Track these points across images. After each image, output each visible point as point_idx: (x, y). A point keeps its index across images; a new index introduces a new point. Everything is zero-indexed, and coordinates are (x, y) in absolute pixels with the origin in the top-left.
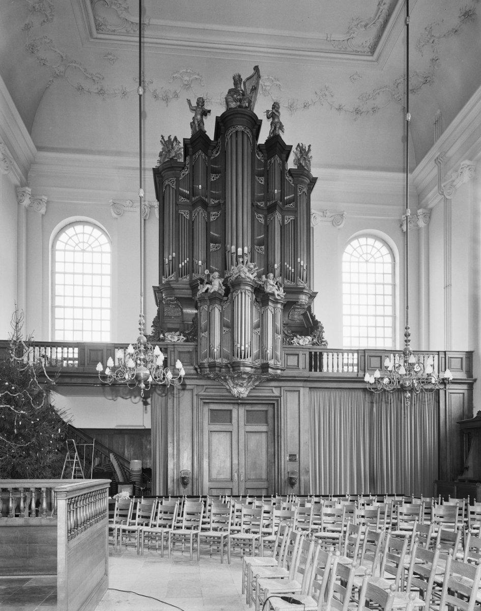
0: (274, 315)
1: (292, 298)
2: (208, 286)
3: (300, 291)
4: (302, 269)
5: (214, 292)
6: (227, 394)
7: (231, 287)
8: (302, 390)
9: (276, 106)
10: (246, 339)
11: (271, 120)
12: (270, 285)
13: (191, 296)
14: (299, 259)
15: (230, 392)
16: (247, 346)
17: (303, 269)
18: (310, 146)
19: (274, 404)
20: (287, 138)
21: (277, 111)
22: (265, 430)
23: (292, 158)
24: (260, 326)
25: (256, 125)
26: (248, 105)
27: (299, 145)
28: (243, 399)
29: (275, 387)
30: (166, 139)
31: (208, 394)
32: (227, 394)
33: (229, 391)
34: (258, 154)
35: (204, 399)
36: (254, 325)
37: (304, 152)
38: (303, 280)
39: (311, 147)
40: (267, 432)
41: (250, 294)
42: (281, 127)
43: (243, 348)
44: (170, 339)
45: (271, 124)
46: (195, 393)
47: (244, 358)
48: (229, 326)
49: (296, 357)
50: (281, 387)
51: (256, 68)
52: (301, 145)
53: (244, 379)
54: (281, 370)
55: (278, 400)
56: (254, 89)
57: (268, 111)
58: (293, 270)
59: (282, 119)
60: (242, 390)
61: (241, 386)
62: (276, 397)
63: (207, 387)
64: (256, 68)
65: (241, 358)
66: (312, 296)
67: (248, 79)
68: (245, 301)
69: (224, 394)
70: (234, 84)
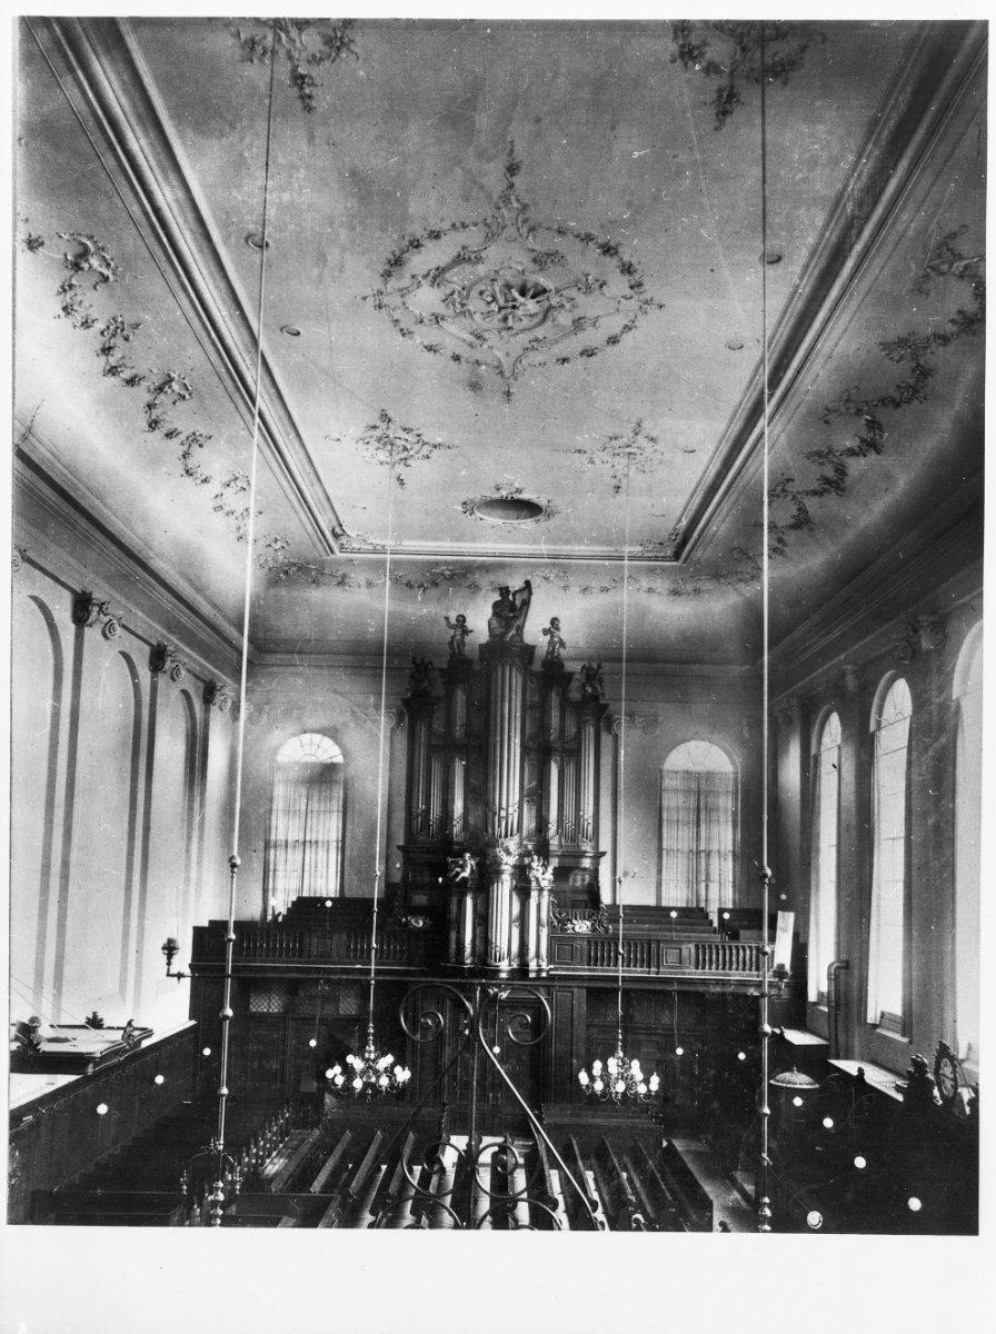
1: (569, 862)
2: (459, 870)
3: (583, 855)
5: (464, 878)
9: (554, 621)
10: (504, 936)
23: (574, 684)
30: (418, 662)
45: (549, 643)
48: (484, 920)
56: (526, 603)
66: (598, 856)
68: (504, 889)
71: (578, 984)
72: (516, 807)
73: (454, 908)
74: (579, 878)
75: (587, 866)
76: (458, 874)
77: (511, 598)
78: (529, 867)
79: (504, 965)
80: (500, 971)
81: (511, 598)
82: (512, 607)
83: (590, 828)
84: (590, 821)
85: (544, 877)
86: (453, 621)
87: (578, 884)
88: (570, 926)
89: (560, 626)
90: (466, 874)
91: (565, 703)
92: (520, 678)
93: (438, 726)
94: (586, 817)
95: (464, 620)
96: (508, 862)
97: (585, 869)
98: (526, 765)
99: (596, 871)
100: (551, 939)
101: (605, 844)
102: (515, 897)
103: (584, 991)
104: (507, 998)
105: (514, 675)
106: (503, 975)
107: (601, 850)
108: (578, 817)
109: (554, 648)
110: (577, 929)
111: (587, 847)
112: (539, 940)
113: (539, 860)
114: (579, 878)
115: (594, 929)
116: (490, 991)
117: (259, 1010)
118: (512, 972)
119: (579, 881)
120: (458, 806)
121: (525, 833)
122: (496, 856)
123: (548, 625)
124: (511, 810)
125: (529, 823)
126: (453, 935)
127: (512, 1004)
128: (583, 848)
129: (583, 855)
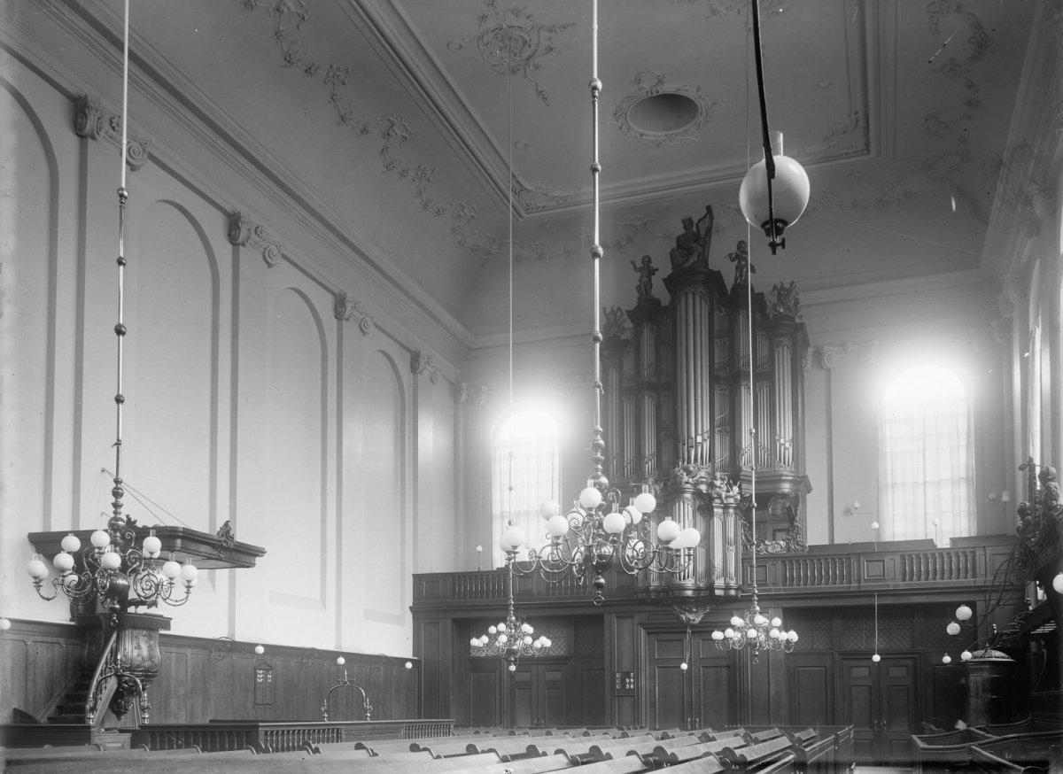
1: (767, 488)
4: (783, 447)
11: (736, 262)
14: (777, 438)
18: (792, 283)
25: (715, 279)
27: (775, 288)
28: (693, 626)
34: (720, 311)
38: (784, 463)
40: (728, 666)
47: (684, 579)
51: (709, 208)
52: (779, 285)
56: (709, 231)
57: (730, 255)
60: (691, 617)
61: (690, 612)
64: (709, 208)
65: (680, 579)
72: (706, 436)
74: (779, 506)
75: (786, 491)
79: (690, 583)
80: (684, 588)
81: (695, 230)
82: (697, 238)
84: (787, 445)
86: (639, 264)
87: (779, 512)
92: (706, 308)
94: (782, 441)
97: (784, 496)
98: (716, 396)
102: (698, 515)
106: (689, 593)
108: (773, 442)
114: (779, 506)
118: (697, 590)
124: (699, 439)
125: (721, 455)
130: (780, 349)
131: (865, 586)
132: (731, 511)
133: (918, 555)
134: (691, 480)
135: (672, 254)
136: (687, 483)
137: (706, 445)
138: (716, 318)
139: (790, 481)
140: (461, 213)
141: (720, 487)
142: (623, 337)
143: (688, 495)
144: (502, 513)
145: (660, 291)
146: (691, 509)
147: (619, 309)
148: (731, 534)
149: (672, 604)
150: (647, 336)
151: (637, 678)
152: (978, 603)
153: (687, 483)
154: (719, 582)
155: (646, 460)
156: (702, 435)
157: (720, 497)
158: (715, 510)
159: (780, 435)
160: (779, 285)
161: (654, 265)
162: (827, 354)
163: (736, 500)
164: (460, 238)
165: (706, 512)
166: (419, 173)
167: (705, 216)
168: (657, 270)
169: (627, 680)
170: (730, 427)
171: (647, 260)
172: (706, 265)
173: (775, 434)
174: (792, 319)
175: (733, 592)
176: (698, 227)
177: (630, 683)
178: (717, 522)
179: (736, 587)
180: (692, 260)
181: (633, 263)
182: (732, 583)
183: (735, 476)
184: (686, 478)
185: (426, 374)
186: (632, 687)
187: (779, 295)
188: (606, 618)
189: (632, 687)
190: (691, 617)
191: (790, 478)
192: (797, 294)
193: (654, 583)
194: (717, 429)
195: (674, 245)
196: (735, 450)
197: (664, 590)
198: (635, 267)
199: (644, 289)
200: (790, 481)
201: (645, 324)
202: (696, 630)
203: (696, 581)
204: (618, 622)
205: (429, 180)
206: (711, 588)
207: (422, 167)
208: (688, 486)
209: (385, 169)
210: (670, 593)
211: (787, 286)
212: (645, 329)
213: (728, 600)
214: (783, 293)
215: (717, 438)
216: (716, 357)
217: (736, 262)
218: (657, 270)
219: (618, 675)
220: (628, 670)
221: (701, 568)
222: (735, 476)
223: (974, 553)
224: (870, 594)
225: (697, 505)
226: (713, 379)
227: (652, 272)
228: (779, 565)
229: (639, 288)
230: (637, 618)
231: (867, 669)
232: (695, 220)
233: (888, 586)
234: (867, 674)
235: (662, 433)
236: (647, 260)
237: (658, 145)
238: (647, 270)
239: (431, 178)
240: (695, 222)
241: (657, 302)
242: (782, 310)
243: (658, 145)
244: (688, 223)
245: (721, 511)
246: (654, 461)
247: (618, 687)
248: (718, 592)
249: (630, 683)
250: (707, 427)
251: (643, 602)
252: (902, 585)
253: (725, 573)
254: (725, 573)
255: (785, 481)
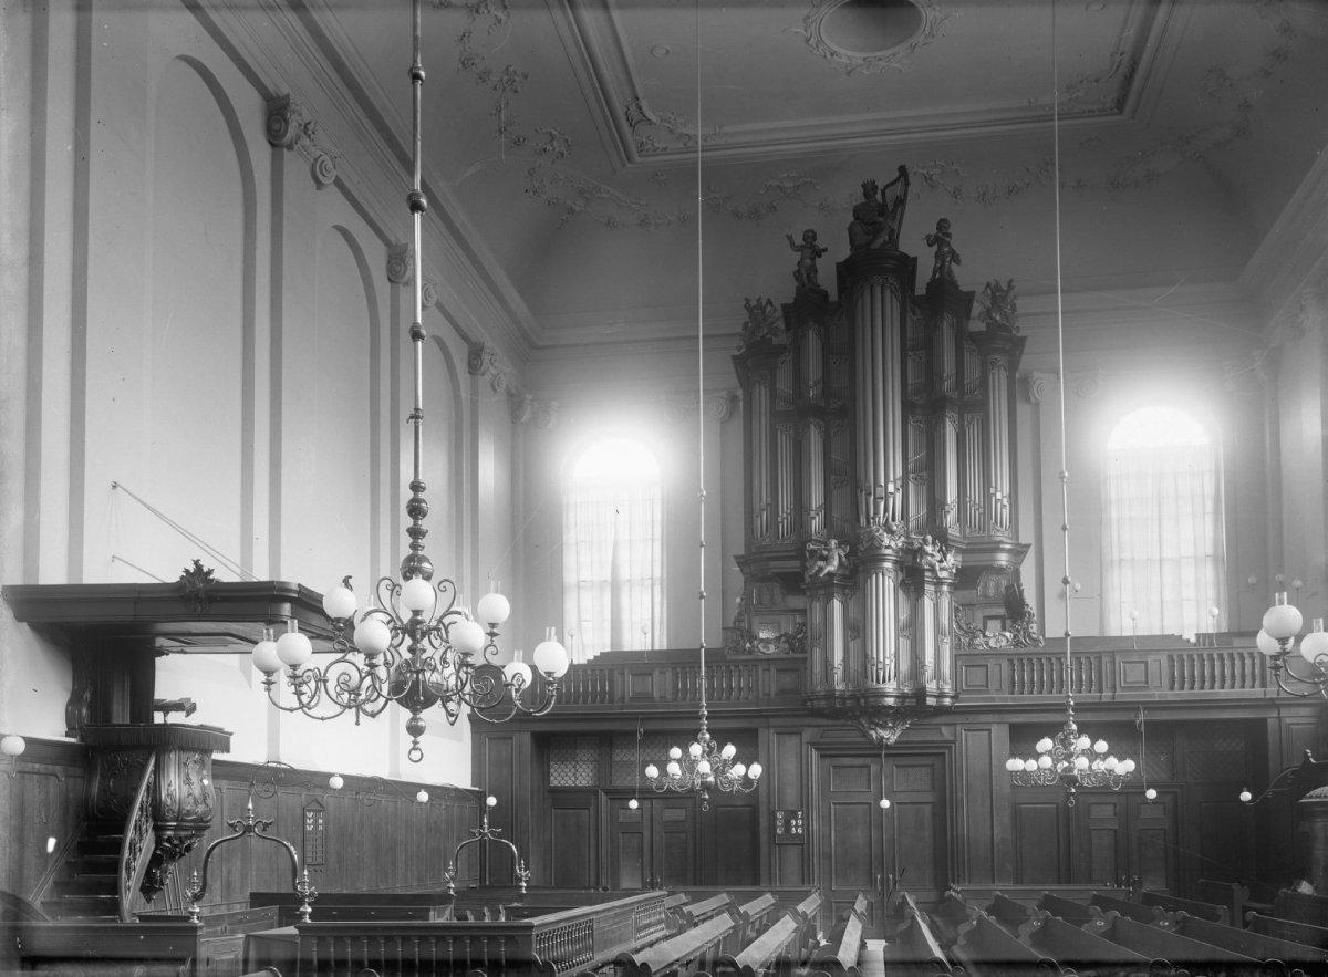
0: (937, 609)
1: (977, 560)
3: (995, 548)
5: (829, 574)
6: (863, 740)
7: (862, 563)
8: (994, 728)
10: (888, 646)
11: (935, 247)
12: (927, 554)
13: (799, 570)
14: (992, 491)
15: (865, 736)
16: (887, 662)
17: (1003, 506)
19: (943, 754)
20: (967, 276)
21: (949, 235)
22: (931, 800)
23: (977, 309)
24: (911, 629)
25: (907, 266)
26: (890, 239)
27: (988, 285)
28: (888, 747)
29: (945, 724)
31: (827, 740)
32: (863, 740)
33: (865, 735)
35: (823, 749)
36: (901, 624)
37: (1000, 295)
38: (1001, 526)
39: (1014, 284)
40: (933, 803)
41: (892, 575)
42: (955, 258)
43: (880, 666)
44: (762, 649)
46: (804, 741)
47: (884, 681)
48: (858, 629)
49: (984, 669)
50: (955, 724)
51: (903, 170)
52: (993, 283)
53: (888, 715)
54: (952, 697)
55: (943, 754)
56: (900, 202)
57: (928, 236)
58: (981, 510)
59: (955, 243)
60: (885, 734)
61: (884, 727)
62: (945, 742)
63: (826, 728)
64: (903, 170)
65: (878, 681)
66: (1019, 552)
67: (887, 186)
68: (885, 589)
69: (859, 739)
70: (865, 194)
71: (996, 717)
72: (899, 483)
73: (817, 619)
75: (1004, 563)
76: (821, 569)
77: (879, 196)
78: (921, 552)
79: (890, 687)
80: (885, 695)
81: (879, 196)
83: (1006, 512)
84: (1005, 501)
85: (945, 564)
86: (799, 241)
87: (991, 592)
88: (980, 640)
89: (950, 231)
90: (832, 567)
91: (962, 336)
92: (897, 306)
93: (784, 384)
94: (999, 496)
95: (814, 238)
96: (891, 545)
97: (1000, 570)
99: (1017, 573)
100: (956, 658)
101: (1027, 536)
102: (900, 592)
103: (1006, 727)
104: (897, 742)
105: (888, 299)
106: (890, 701)
107: (1023, 541)
109: (943, 262)
110: (992, 643)
111: (1002, 536)
112: (937, 656)
113: (934, 544)
115: (1017, 643)
116: (873, 733)
117: (563, 783)
118: (901, 697)
119: (992, 586)
120: (816, 498)
121: (912, 524)
122: (872, 538)
123: (934, 232)
124: (891, 488)
125: (917, 511)
126: (817, 654)
127: (898, 753)
128: (998, 539)
129: (995, 548)
130: (996, 371)
131: (1121, 696)
132: (945, 588)
133: (1192, 656)
134: (893, 544)
135: (851, 229)
136: (888, 547)
137: (899, 496)
138: (909, 323)
139: (1009, 551)
140: (549, 147)
141: (932, 556)
142: (775, 341)
143: (888, 565)
144: (578, 582)
145: (827, 278)
146: (892, 585)
147: (769, 302)
148: (945, 620)
149: (860, 716)
150: (813, 343)
151: (806, 818)
152: (1269, 720)
153: (888, 547)
154: (931, 686)
155: (812, 513)
156: (895, 481)
157: (933, 569)
158: (927, 587)
159: (996, 488)
160: (993, 283)
161: (820, 243)
162: (1037, 383)
163: (951, 573)
164: (537, 184)
165: (912, 588)
166: (505, 78)
167: (898, 179)
168: (825, 250)
169: (794, 822)
170: (927, 473)
171: (810, 236)
172: (897, 248)
173: (990, 486)
174: (1008, 329)
175: (947, 701)
176: (883, 193)
177: (797, 827)
178: (928, 603)
179: (952, 693)
180: (881, 240)
181: (790, 238)
182: (947, 688)
183: (942, 538)
184: (886, 541)
185: (487, 377)
186: (800, 831)
187: (994, 297)
188: (762, 734)
189: (800, 831)
190: (885, 734)
191: (1008, 546)
192: (1015, 297)
193: (839, 687)
194: (911, 475)
195: (852, 219)
196: (935, 504)
197: (853, 697)
198: (792, 244)
199: (805, 276)
200: (1009, 551)
201: (811, 323)
202: (891, 752)
203: (898, 683)
204: (779, 743)
205: (516, 91)
206: (920, 694)
207: (511, 69)
208: (889, 551)
209: (461, 66)
210: (862, 701)
211: (1004, 286)
212: (811, 331)
213: (940, 710)
214: (998, 294)
215: (911, 486)
216: (910, 375)
217: (935, 247)
218: (825, 250)
219: (779, 815)
220: (793, 809)
221: (905, 667)
222: (942, 538)
223: (1100, 659)
224: (1133, 707)
225: (900, 578)
226: (908, 408)
227: (818, 253)
228: (1005, 665)
229: (797, 275)
230: (808, 734)
231: (1111, 808)
232: (881, 184)
233: (993, 699)
234: (1112, 813)
235: (833, 477)
236: (810, 236)
237: (849, 73)
238: (811, 247)
239: (519, 89)
240: (881, 187)
241: (825, 295)
242: (998, 318)
243: (849, 73)
244: (869, 189)
245: (932, 588)
246: (822, 514)
247: (779, 831)
248: (931, 701)
249: (797, 827)
250: (899, 473)
251: (818, 713)
252: (1170, 696)
253: (938, 675)
254: (938, 675)
255: (1003, 550)
